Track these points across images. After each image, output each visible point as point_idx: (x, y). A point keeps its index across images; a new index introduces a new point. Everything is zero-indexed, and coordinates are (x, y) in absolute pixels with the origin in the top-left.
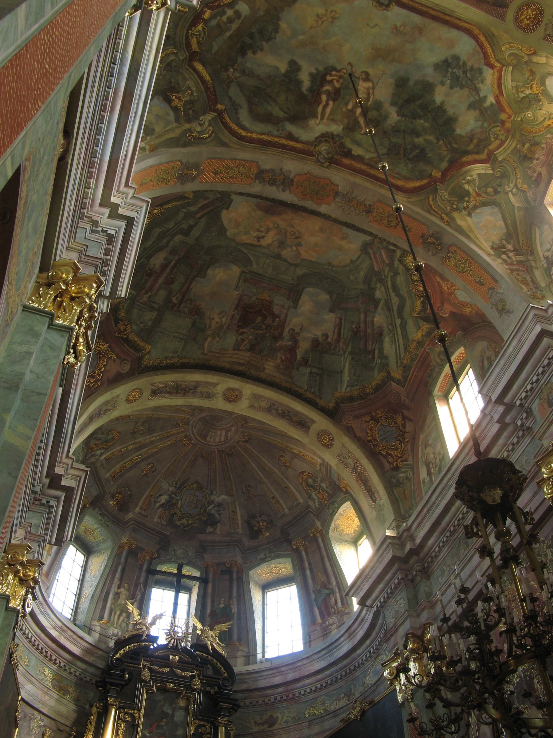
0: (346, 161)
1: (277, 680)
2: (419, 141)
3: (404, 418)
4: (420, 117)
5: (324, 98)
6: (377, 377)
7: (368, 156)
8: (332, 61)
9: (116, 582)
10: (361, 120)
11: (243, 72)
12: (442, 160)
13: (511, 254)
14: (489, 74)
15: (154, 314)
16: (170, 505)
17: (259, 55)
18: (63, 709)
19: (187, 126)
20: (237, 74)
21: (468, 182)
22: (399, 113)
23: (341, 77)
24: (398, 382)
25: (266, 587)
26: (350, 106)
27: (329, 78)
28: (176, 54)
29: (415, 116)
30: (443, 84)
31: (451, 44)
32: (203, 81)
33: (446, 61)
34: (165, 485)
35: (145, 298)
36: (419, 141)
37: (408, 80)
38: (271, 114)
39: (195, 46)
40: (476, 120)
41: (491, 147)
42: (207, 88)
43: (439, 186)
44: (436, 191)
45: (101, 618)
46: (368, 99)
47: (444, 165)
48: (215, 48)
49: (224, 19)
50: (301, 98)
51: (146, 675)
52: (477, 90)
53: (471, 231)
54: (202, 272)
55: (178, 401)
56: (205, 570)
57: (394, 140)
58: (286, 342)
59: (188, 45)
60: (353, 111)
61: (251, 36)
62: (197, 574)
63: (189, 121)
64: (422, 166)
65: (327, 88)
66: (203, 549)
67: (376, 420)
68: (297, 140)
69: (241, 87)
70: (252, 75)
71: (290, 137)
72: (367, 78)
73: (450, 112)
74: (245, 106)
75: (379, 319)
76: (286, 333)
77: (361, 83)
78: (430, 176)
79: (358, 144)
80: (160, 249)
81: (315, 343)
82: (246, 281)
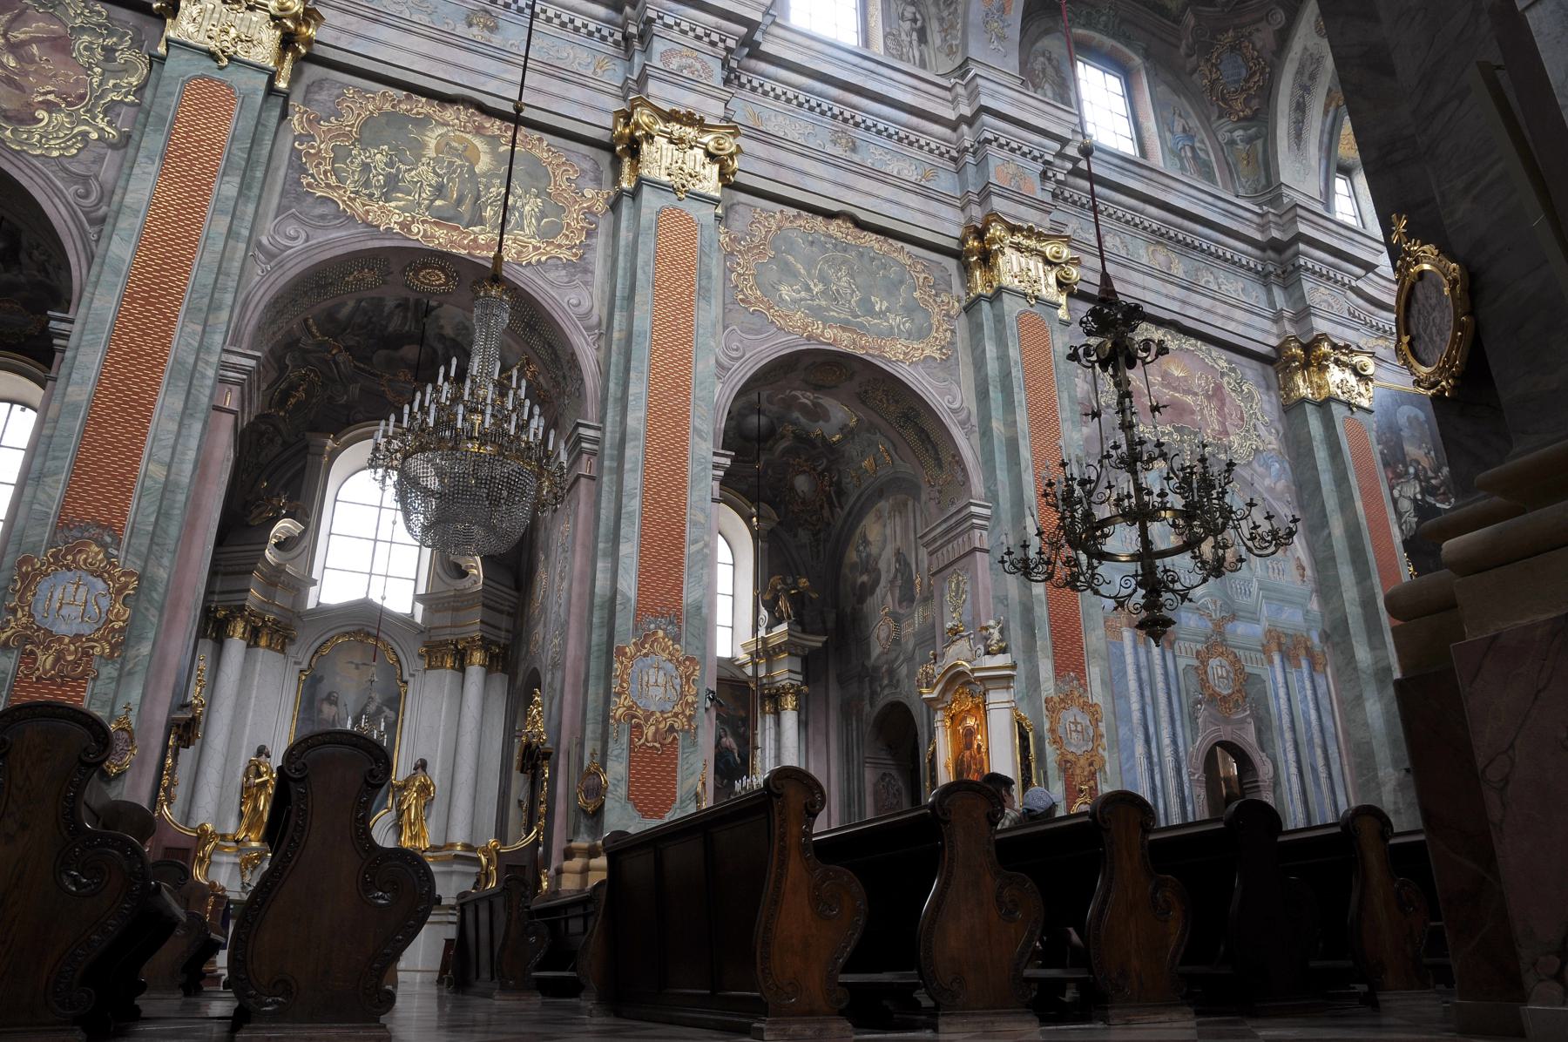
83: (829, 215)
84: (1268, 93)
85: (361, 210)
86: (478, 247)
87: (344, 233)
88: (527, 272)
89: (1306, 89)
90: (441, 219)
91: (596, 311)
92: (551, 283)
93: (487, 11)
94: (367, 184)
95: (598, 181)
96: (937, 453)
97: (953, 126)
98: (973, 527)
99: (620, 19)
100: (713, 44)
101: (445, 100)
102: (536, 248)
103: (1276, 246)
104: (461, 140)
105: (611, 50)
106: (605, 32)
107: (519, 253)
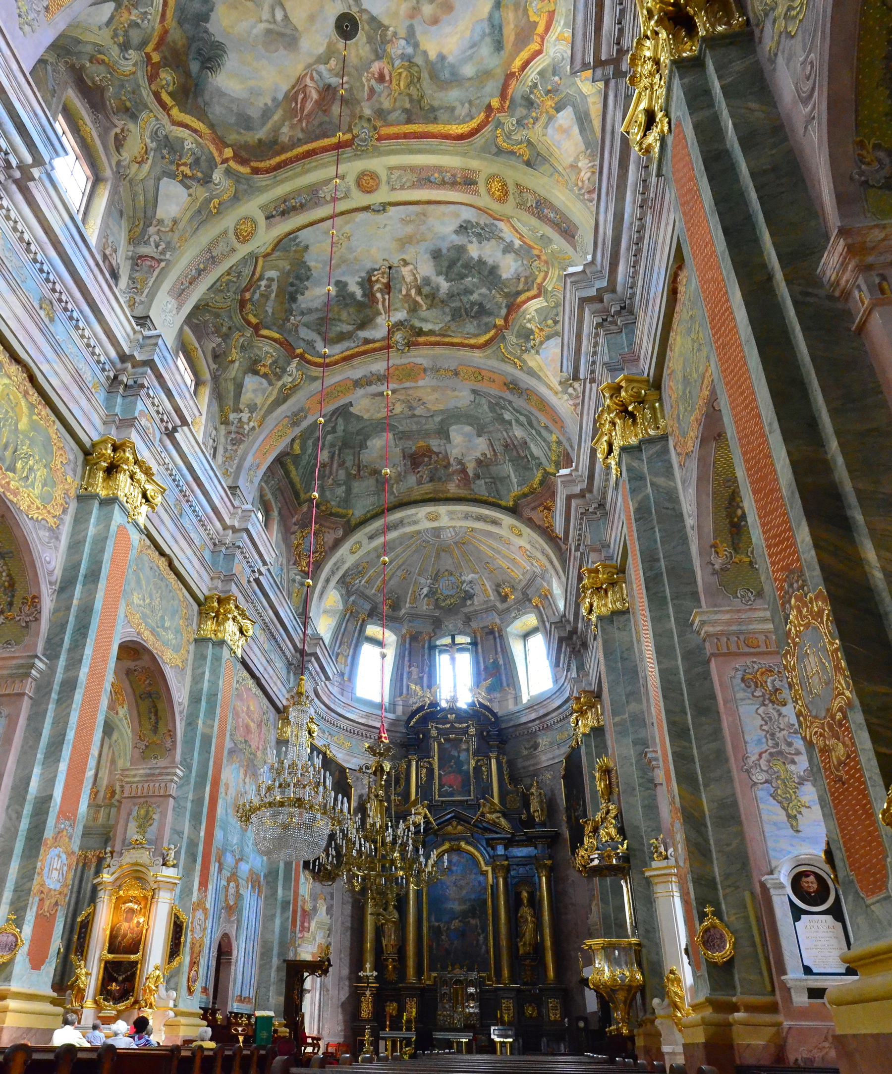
5: (379, 295)
8: (369, 266)
10: (419, 299)
11: (303, 314)
17: (307, 293)
19: (280, 383)
20: (299, 318)
22: (448, 280)
23: (383, 273)
26: (404, 292)
27: (374, 279)
28: (243, 335)
31: (457, 215)
32: (275, 340)
38: (342, 333)
39: (254, 320)
42: (281, 344)
46: (416, 279)
48: (270, 311)
49: (263, 288)
57: (453, 305)
59: (249, 323)
60: (408, 295)
61: (292, 285)
63: (279, 378)
65: (377, 286)
70: (310, 311)
72: (406, 263)
77: (403, 269)
86: (9, 490)
88: (30, 523)
91: (56, 572)
92: (40, 539)
93: (51, 303)
101: (15, 358)
102: (38, 508)
104: (16, 397)
107: (29, 507)
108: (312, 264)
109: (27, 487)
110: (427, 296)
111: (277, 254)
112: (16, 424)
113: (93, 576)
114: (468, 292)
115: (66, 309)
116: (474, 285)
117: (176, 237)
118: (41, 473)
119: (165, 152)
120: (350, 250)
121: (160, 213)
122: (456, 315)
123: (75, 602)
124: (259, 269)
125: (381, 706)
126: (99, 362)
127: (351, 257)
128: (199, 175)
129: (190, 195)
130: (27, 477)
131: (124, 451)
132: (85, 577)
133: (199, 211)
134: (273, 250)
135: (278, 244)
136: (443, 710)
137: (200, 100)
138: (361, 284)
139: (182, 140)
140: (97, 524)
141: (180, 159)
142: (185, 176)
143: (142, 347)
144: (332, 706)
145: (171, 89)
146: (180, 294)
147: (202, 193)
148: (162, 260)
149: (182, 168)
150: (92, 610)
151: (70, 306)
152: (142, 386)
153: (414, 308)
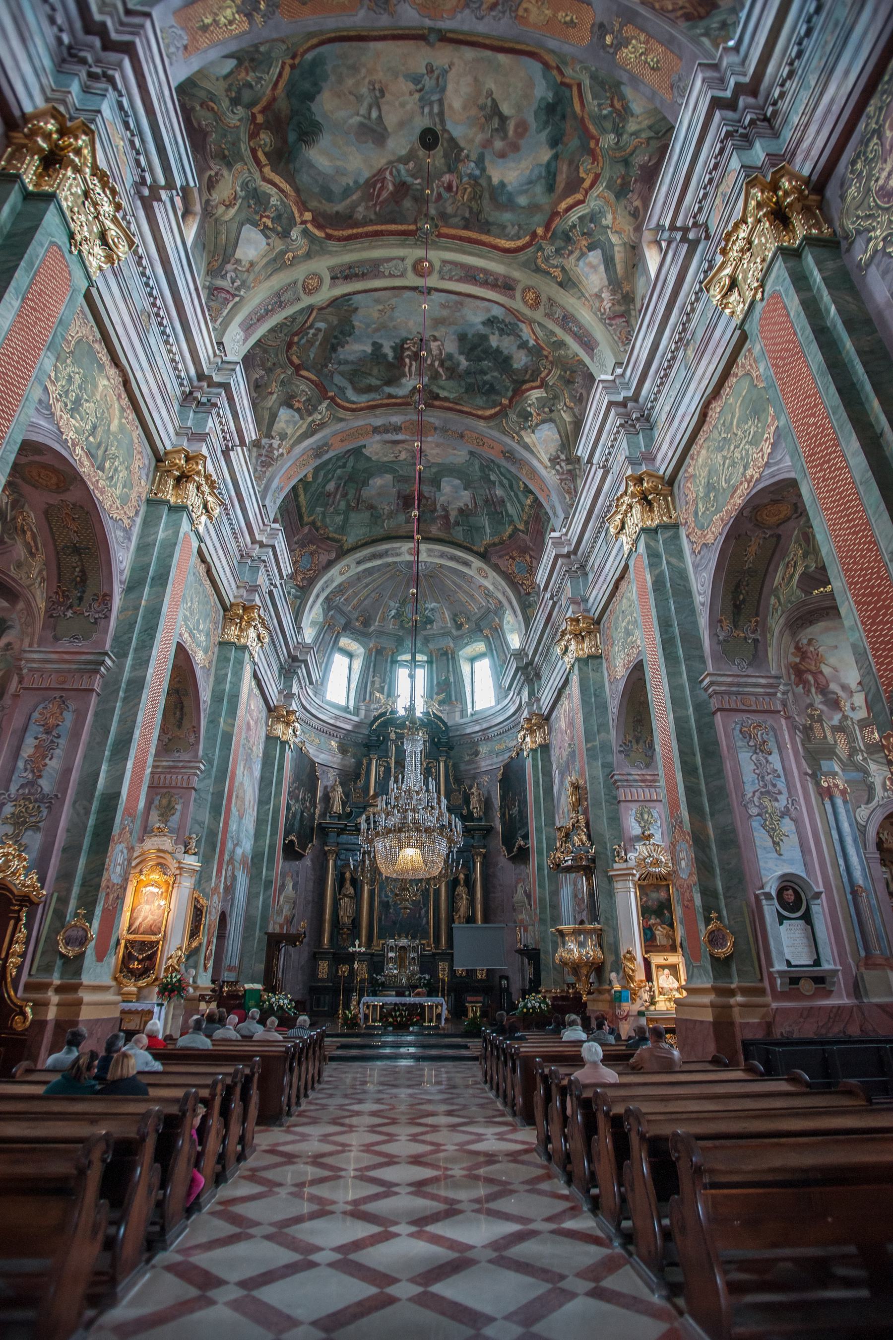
0: (437, 403)
1: (477, 728)
2: (487, 378)
3: (531, 557)
4: (484, 360)
5: (407, 360)
6: (509, 530)
7: (452, 396)
8: (404, 334)
9: (371, 673)
10: (440, 370)
12: (507, 390)
13: (563, 464)
14: (523, 326)
15: (342, 517)
16: (399, 615)
18: (347, 763)
21: (530, 405)
24: (523, 532)
25: (472, 660)
29: (480, 360)
30: (493, 334)
33: (489, 320)
34: (392, 604)
35: (332, 509)
36: (487, 378)
37: (466, 335)
40: (527, 356)
41: (543, 375)
43: (509, 411)
44: (507, 415)
45: (365, 699)
47: (510, 394)
50: (390, 366)
51: (393, 736)
52: (520, 337)
53: (535, 446)
54: (365, 483)
55: (378, 562)
56: (430, 655)
57: (469, 381)
58: (440, 512)
60: (432, 365)
62: (425, 658)
64: (494, 397)
65: (407, 353)
66: (427, 640)
67: (514, 559)
68: (396, 397)
69: (342, 374)
71: (390, 396)
72: (435, 339)
73: (506, 352)
74: (349, 387)
75: (499, 492)
76: (438, 507)
78: (501, 404)
79: (444, 389)
80: (330, 480)
81: (461, 511)
82: (399, 481)
83: (204, 561)
84: (312, 581)
85: (59, 413)
86: (97, 488)
87: (46, 425)
89: (323, 590)
90: (90, 454)
93: (149, 316)
94: (67, 393)
95: (147, 476)
96: (182, 718)
97: (254, 541)
98: (195, 774)
99: (196, 383)
100: (225, 438)
101: (116, 362)
103: (295, 659)
105: (178, 393)
106: (185, 383)
108: (356, 323)
109: (110, 487)
110: (447, 369)
111: (329, 310)
112: (109, 426)
113: (162, 579)
114: (483, 372)
115: (160, 324)
116: (489, 368)
117: (251, 277)
118: (123, 474)
119: (252, 202)
120: (391, 319)
121: (239, 254)
122: (470, 389)
123: (143, 603)
124: (311, 318)
125: (346, 709)
126: (179, 377)
127: (391, 325)
128: (279, 229)
129: (268, 244)
130: (112, 477)
131: (197, 464)
132: (153, 579)
133: (275, 260)
134: (328, 306)
135: (334, 302)
136: (400, 718)
137: (291, 166)
138: (394, 349)
139: (270, 196)
140: (165, 530)
141: (265, 211)
142: (266, 227)
143: (219, 369)
144: (308, 707)
145: (267, 149)
146: (248, 328)
147: (279, 245)
148: (237, 296)
149: (264, 220)
150: (159, 612)
151: (165, 322)
152: (215, 405)
153: (435, 376)
